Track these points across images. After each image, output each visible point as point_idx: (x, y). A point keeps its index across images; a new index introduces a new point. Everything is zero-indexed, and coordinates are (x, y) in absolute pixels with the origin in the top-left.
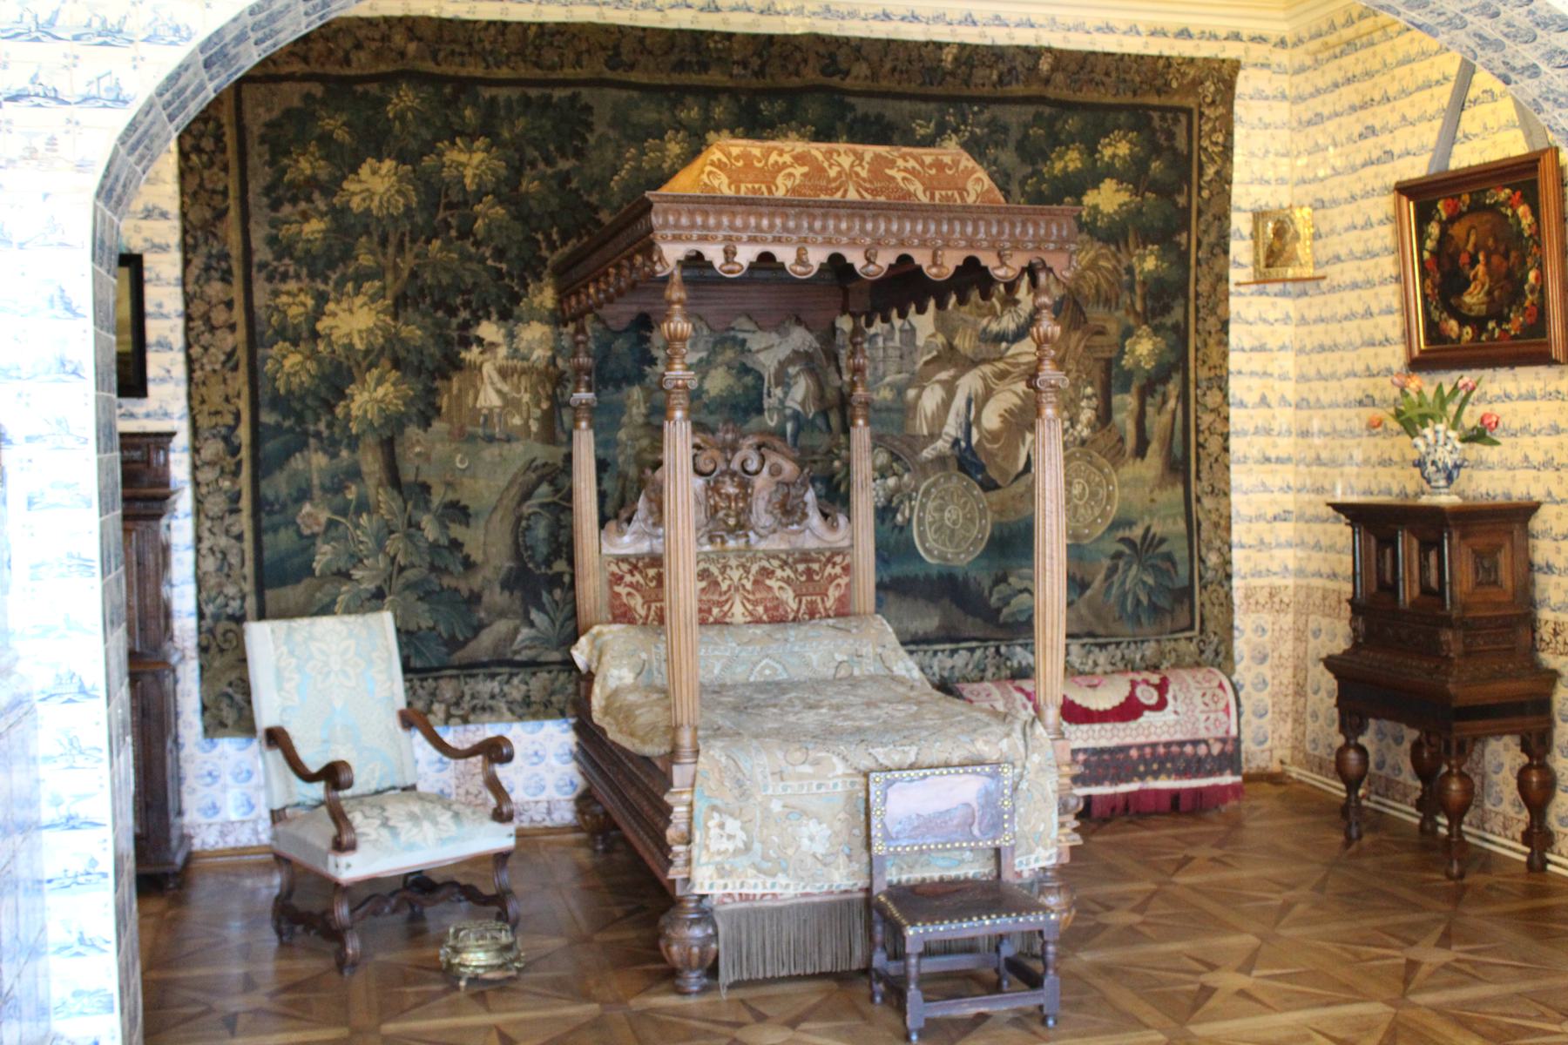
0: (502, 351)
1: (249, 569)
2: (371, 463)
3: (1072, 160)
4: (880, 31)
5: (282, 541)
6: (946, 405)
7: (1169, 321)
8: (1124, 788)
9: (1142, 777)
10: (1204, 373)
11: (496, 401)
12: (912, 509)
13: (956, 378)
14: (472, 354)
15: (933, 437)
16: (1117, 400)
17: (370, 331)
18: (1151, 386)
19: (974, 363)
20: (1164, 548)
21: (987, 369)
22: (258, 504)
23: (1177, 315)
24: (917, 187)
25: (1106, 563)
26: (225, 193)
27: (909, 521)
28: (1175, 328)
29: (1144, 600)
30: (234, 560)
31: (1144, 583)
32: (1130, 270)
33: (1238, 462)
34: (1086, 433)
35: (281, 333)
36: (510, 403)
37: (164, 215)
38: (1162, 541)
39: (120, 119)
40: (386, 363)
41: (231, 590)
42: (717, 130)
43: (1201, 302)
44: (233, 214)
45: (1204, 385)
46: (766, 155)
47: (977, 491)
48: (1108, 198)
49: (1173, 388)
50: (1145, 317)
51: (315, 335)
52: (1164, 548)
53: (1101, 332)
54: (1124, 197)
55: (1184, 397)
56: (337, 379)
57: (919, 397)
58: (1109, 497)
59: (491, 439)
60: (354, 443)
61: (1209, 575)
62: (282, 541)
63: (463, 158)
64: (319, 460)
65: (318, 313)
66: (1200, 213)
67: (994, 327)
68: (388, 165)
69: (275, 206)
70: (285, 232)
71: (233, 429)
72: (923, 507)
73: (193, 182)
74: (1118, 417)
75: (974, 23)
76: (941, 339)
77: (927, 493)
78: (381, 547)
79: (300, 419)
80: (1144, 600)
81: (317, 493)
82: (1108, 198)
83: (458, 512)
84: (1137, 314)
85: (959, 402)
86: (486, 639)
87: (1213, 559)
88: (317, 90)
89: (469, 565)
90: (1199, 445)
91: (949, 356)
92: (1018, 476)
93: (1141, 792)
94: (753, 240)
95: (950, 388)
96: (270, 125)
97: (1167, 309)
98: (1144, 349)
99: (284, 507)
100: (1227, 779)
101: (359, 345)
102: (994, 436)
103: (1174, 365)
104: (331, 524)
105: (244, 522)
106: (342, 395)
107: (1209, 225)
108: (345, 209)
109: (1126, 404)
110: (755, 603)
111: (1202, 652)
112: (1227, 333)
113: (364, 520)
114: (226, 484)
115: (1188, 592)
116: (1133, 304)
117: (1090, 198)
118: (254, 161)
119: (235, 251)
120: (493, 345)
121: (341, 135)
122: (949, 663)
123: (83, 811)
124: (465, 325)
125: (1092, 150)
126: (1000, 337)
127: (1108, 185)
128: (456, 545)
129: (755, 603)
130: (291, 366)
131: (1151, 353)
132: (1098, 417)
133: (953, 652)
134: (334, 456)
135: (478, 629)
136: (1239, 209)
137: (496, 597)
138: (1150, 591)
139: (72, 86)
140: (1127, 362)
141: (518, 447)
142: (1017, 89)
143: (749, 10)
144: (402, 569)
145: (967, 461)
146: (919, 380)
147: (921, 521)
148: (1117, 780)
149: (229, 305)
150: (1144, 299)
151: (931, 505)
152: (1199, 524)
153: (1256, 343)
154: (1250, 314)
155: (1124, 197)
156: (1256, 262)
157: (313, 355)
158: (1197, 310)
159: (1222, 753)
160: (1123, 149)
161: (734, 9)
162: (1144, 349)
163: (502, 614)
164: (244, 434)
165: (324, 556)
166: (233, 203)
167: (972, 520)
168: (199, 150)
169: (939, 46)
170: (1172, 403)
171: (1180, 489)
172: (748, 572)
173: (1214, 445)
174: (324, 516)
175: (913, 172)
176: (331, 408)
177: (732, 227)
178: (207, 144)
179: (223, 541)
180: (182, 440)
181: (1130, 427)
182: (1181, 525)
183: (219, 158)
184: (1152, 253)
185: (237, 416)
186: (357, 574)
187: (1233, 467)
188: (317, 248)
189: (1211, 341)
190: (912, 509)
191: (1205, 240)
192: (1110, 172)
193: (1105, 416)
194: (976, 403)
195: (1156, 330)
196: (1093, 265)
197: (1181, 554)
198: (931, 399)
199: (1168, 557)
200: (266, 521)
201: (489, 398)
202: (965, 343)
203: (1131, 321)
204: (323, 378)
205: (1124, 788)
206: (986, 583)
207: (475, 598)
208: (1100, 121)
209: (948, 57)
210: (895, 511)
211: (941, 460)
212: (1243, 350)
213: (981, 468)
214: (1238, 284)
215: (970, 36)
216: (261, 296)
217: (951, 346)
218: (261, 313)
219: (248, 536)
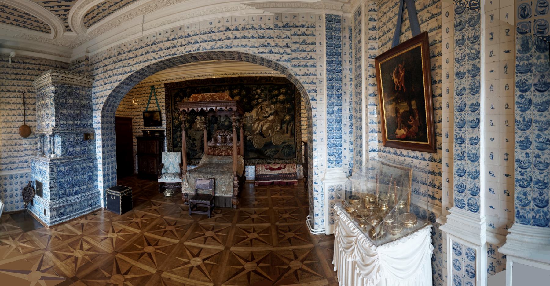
3: (276, 92)
5: (175, 142)
6: (258, 126)
14: (196, 120)
15: (256, 130)
23: (292, 113)
36: (201, 126)
48: (282, 97)
49: (292, 124)
50: (287, 113)
55: (294, 124)
82: (282, 97)
83: (194, 140)
85: (260, 126)
86: (197, 155)
87: (299, 148)
89: (196, 146)
95: (259, 124)
98: (287, 118)
102: (265, 130)
103: (292, 119)
105: (171, 140)
109: (285, 126)
117: (279, 97)
125: (279, 91)
127: (282, 96)
128: (194, 144)
130: (176, 122)
135: (197, 154)
142: (268, 82)
145: (261, 134)
146: (254, 123)
160: (284, 90)
162: (287, 118)
173: (299, 131)
181: (285, 129)
192: (282, 94)
193: (281, 128)
194: (262, 126)
196: (279, 107)
198: (256, 125)
199: (292, 147)
201: (198, 126)
202: (261, 118)
207: (196, 150)
208: (280, 87)
209: (258, 79)
211: (257, 134)
215: (261, 75)
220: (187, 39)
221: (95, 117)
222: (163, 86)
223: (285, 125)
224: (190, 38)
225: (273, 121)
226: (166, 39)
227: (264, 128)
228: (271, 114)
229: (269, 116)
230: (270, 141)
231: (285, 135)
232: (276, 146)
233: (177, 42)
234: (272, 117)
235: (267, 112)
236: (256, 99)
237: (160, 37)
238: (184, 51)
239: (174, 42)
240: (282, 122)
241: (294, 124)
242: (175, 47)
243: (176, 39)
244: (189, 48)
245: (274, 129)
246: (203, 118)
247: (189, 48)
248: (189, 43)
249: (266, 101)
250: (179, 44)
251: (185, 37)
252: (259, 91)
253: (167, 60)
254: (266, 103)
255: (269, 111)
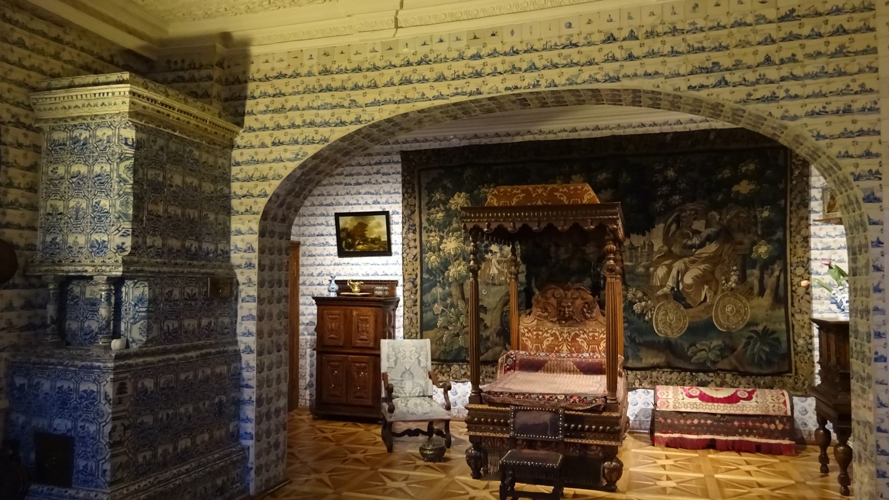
0: (499, 255)
1: (419, 324)
2: (455, 291)
3: (727, 173)
4: (641, 131)
5: (428, 316)
6: (668, 274)
7: (775, 237)
8: (730, 438)
9: (740, 435)
10: (794, 260)
11: (496, 272)
12: (652, 315)
13: (672, 263)
14: (489, 256)
15: (662, 286)
16: (748, 272)
17: (456, 248)
18: (766, 265)
19: (680, 257)
20: (775, 336)
21: (686, 259)
22: (422, 303)
23: (779, 234)
24: (564, 199)
25: (744, 341)
26: (415, 205)
27: (651, 319)
28: (778, 240)
29: (764, 357)
30: (414, 321)
31: (764, 351)
32: (755, 217)
33: (816, 299)
34: (734, 285)
35: (430, 249)
37: (398, 213)
38: (774, 332)
39: (266, 200)
40: (461, 259)
41: (413, 331)
42: (576, 174)
43: (793, 229)
44: (417, 212)
45: (795, 265)
46: (512, 191)
47: (682, 308)
48: (744, 188)
49: (777, 268)
51: (440, 250)
52: (775, 336)
53: (741, 243)
54: (753, 187)
56: (445, 264)
57: (655, 270)
58: (746, 313)
59: (494, 285)
60: (450, 284)
61: (799, 349)
62: (428, 316)
63: (487, 190)
64: (440, 290)
65: (441, 243)
66: (791, 191)
67: (689, 243)
68: (463, 194)
69: (429, 209)
70: (432, 217)
71: (415, 279)
72: (657, 314)
73: (405, 202)
74: (749, 279)
75: (681, 123)
76: (666, 248)
77: (659, 308)
78: (458, 319)
79: (435, 277)
80: (764, 357)
81: (439, 301)
82: (744, 188)
84: (758, 235)
85: (674, 272)
87: (801, 342)
88: (442, 171)
89: (486, 327)
90: (792, 291)
91: (669, 255)
92: (701, 303)
93: (740, 441)
94: (496, 221)
96: (428, 184)
97: (774, 233)
98: (763, 250)
99: (429, 305)
100: (786, 442)
101: (452, 253)
102: (690, 286)
103: (780, 254)
104: (443, 311)
106: (447, 269)
107: (796, 196)
108: (450, 209)
110: (571, 347)
111: (796, 383)
112: (808, 242)
113: (453, 310)
114: (412, 297)
115: (787, 356)
116: (757, 231)
117: (735, 188)
118: (423, 195)
119: (417, 224)
120: (496, 253)
121: (449, 185)
122: (670, 376)
123: (250, 383)
124: (487, 246)
126: (692, 246)
127: (744, 183)
129: (571, 347)
130: (432, 259)
131: (766, 252)
132: (739, 279)
133: (671, 373)
134: (444, 289)
136: (814, 188)
137: (494, 338)
138: (767, 354)
139: (256, 192)
140: (754, 255)
141: (503, 288)
143: (588, 130)
144: (464, 327)
147: (656, 319)
148: (727, 434)
149: (415, 240)
150: (762, 229)
151: (661, 313)
152: (793, 326)
153: (825, 246)
154: (822, 233)
155: (753, 187)
156: (824, 210)
157: (439, 256)
158: (791, 233)
159: (783, 429)
160: (752, 167)
161: (582, 130)
162: (763, 250)
163: (496, 345)
164: (418, 281)
165: (440, 321)
166: (417, 208)
167: (680, 320)
168: (407, 192)
169: (665, 134)
170: (777, 273)
171: (783, 310)
172: (570, 334)
174: (441, 308)
175: (564, 193)
176: (443, 273)
177: (488, 217)
178: (410, 191)
179: (411, 315)
180: (401, 282)
181: (756, 283)
182: (784, 326)
183: (413, 195)
184: (767, 209)
185: (417, 275)
186: (450, 328)
187: (814, 301)
188: (441, 222)
189: (798, 246)
190: (652, 315)
191: (795, 202)
192: (745, 176)
193: (743, 279)
194: (682, 273)
195: (769, 242)
196: (737, 216)
197: (784, 338)
198: (661, 271)
199: (777, 340)
200: (424, 309)
201: (494, 271)
202: (676, 249)
203: (756, 238)
204: (442, 263)
205: (730, 438)
206: (686, 346)
207: (488, 338)
209: (669, 138)
210: (645, 315)
211: (665, 296)
212: (817, 249)
213: (684, 299)
214: (815, 221)
216: (424, 239)
217: (670, 251)
218: (424, 243)
219: (419, 313)
220: (508, 59)
221: (239, 232)
222: (398, 158)
223: (756, 272)
224: (516, 58)
225: (715, 260)
226: (456, 55)
227: (688, 279)
228: (709, 239)
229: (702, 245)
230: (705, 317)
231: (756, 301)
232: (729, 334)
233: (484, 64)
234: (712, 248)
235: (697, 232)
236: (661, 196)
237: (441, 49)
238: (501, 87)
239: (477, 64)
240: (746, 262)
241: (784, 270)
242: (478, 75)
243: (480, 57)
244: (512, 80)
245: (717, 281)
246: (507, 249)
247: (512, 80)
248: (514, 69)
249: (693, 200)
250: (488, 70)
251: (505, 54)
252: (671, 173)
253: (455, 104)
254: (690, 206)
255: (702, 229)
